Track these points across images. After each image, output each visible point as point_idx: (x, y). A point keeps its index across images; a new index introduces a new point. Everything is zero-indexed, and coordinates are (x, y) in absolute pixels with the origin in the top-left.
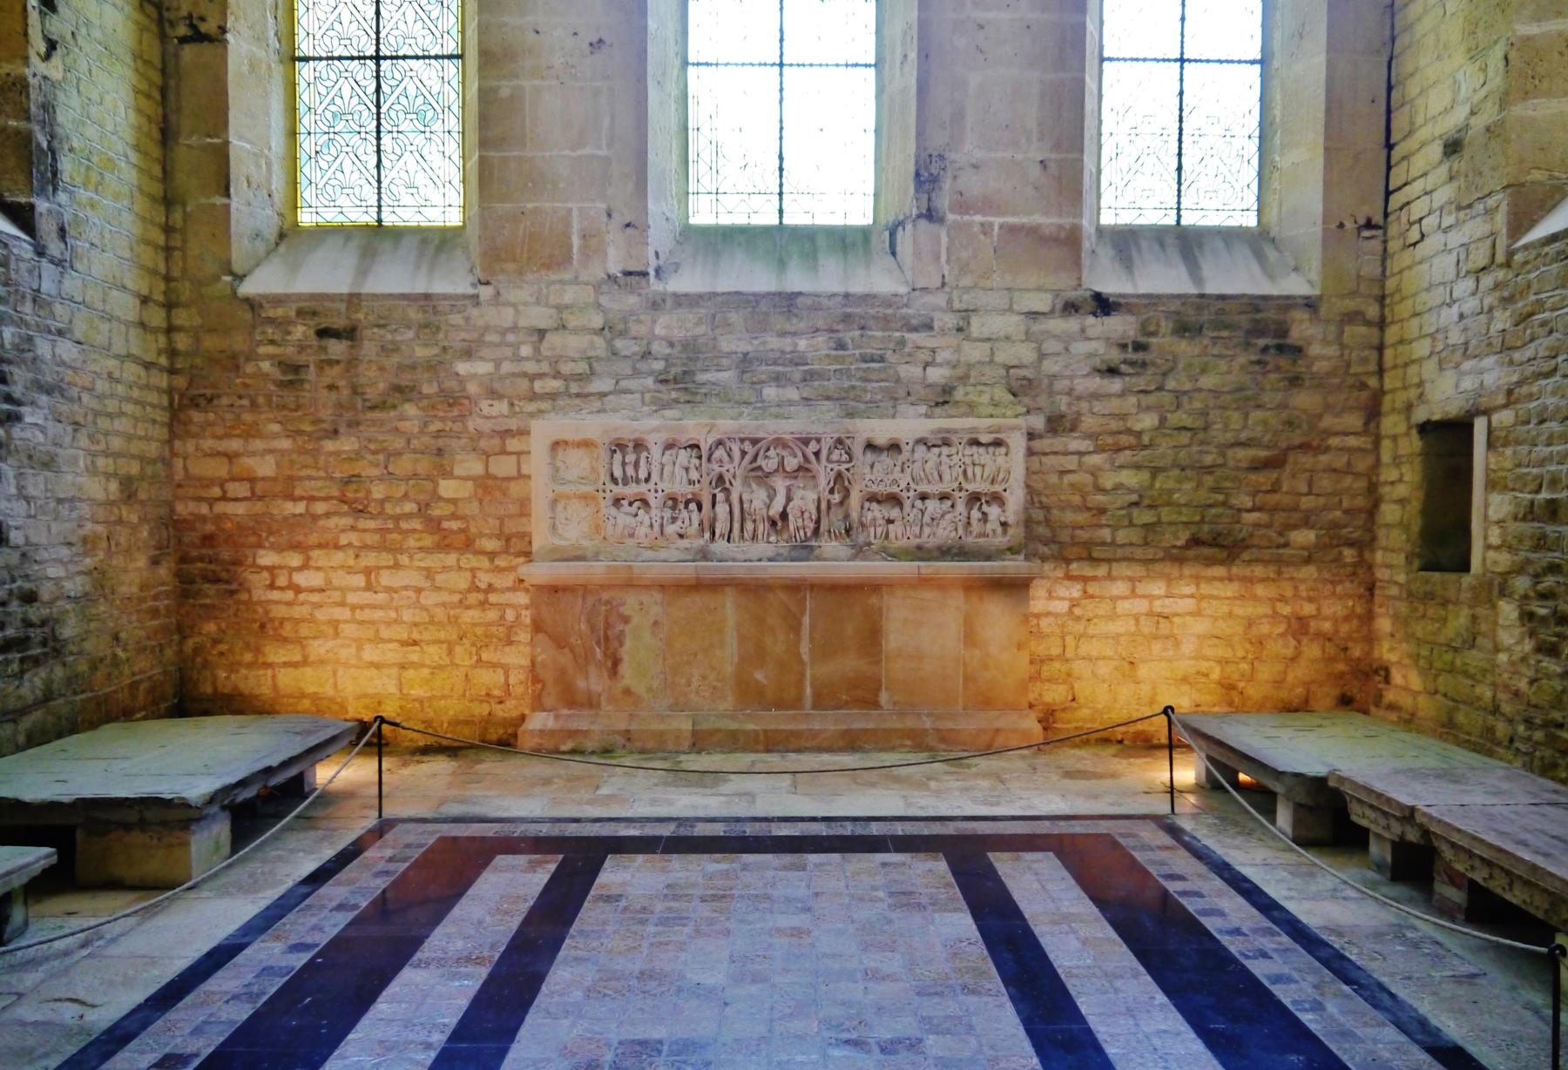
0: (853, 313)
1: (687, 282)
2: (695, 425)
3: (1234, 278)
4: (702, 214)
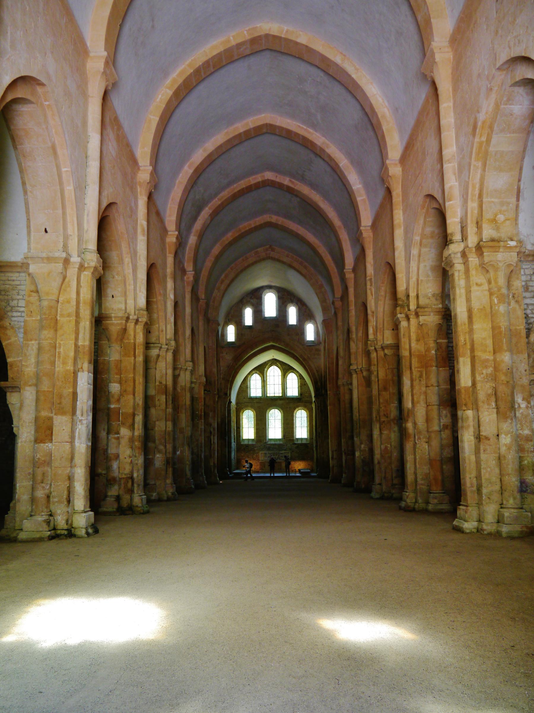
0: (280, 445)
1: (269, 443)
2: (270, 452)
3: (304, 442)
4: (270, 438)
